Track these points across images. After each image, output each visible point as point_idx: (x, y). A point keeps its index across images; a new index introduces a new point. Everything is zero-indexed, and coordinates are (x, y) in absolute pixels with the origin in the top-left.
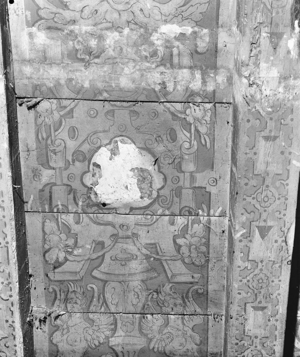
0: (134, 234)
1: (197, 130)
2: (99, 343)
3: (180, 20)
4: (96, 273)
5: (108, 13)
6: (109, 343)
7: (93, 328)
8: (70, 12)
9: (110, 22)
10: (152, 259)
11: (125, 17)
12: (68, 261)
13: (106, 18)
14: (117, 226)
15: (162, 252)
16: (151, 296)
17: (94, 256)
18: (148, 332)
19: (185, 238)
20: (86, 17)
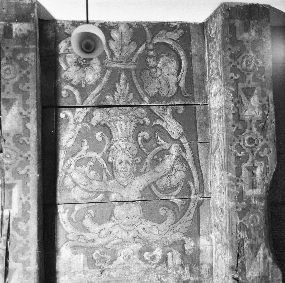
3: (172, 233)
5: (119, 233)
8: (91, 234)
9: (120, 239)
11: (131, 235)
13: (118, 236)
20: (102, 236)
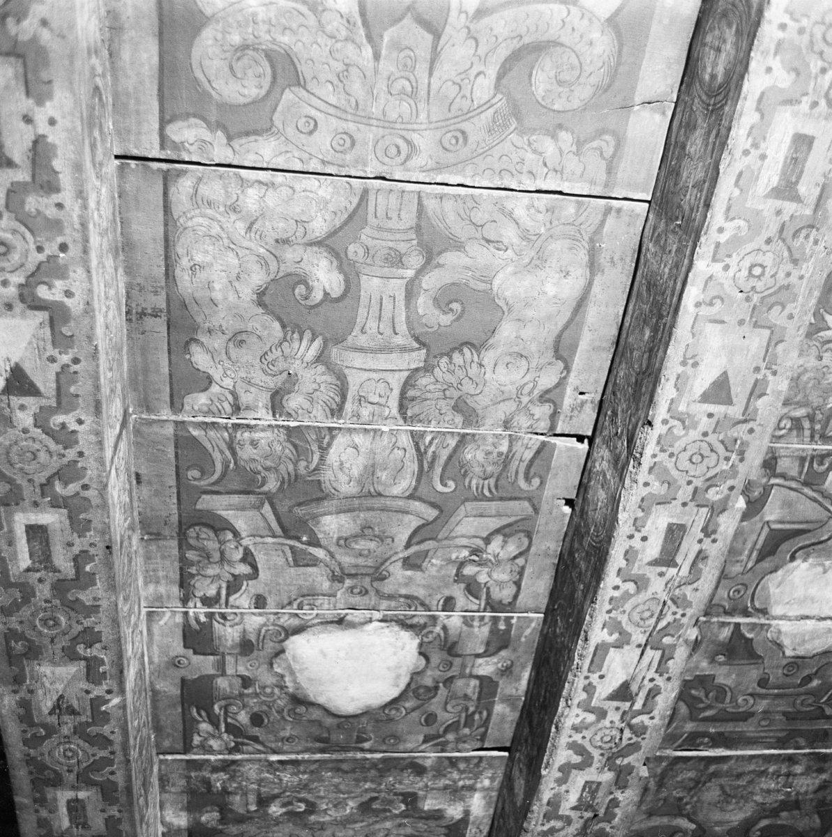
0: (341, 581)
1: (217, 726)
2: (451, 358)
4: (431, 513)
6: (428, 355)
7: (460, 393)
10: (304, 539)
12: (485, 536)
14: (372, 593)
15: (283, 551)
16: (312, 466)
17: (429, 545)
18: (324, 378)
19: (233, 575)
